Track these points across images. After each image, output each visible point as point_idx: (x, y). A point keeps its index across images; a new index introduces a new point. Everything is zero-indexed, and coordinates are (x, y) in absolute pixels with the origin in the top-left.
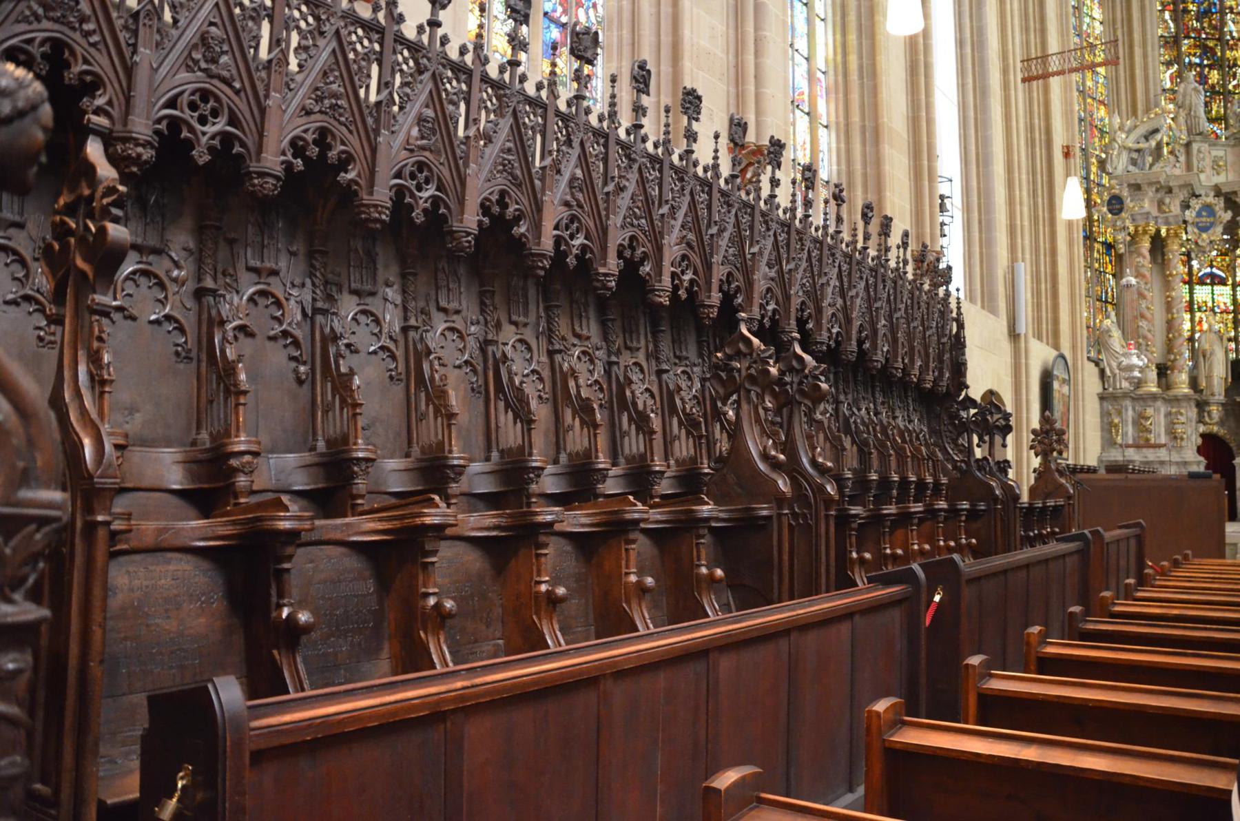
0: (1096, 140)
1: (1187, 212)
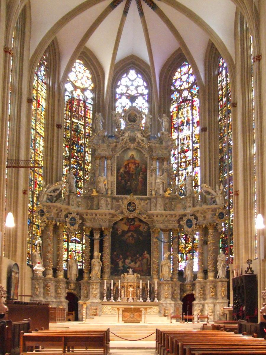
0: (37, 188)
1: (67, 219)
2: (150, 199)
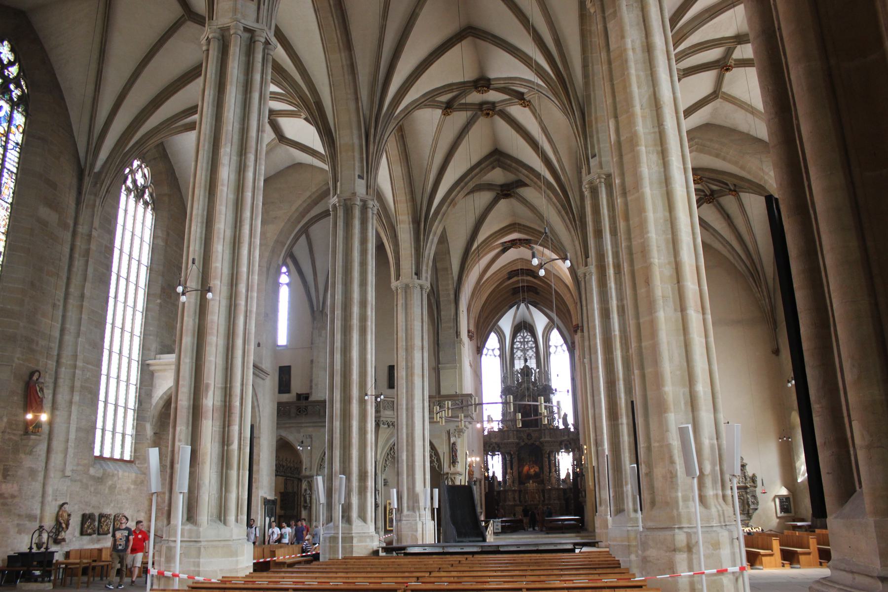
2: (540, 430)
